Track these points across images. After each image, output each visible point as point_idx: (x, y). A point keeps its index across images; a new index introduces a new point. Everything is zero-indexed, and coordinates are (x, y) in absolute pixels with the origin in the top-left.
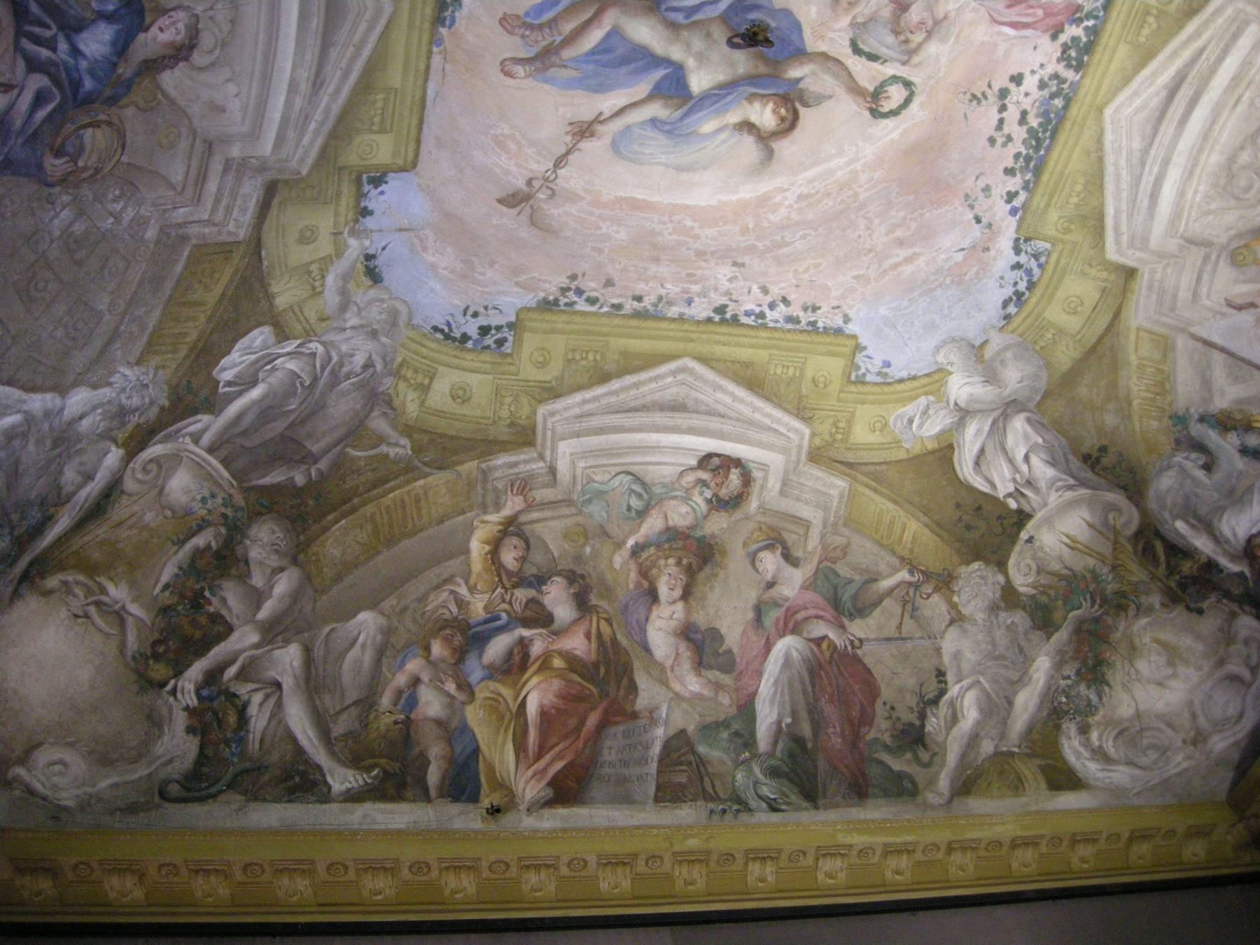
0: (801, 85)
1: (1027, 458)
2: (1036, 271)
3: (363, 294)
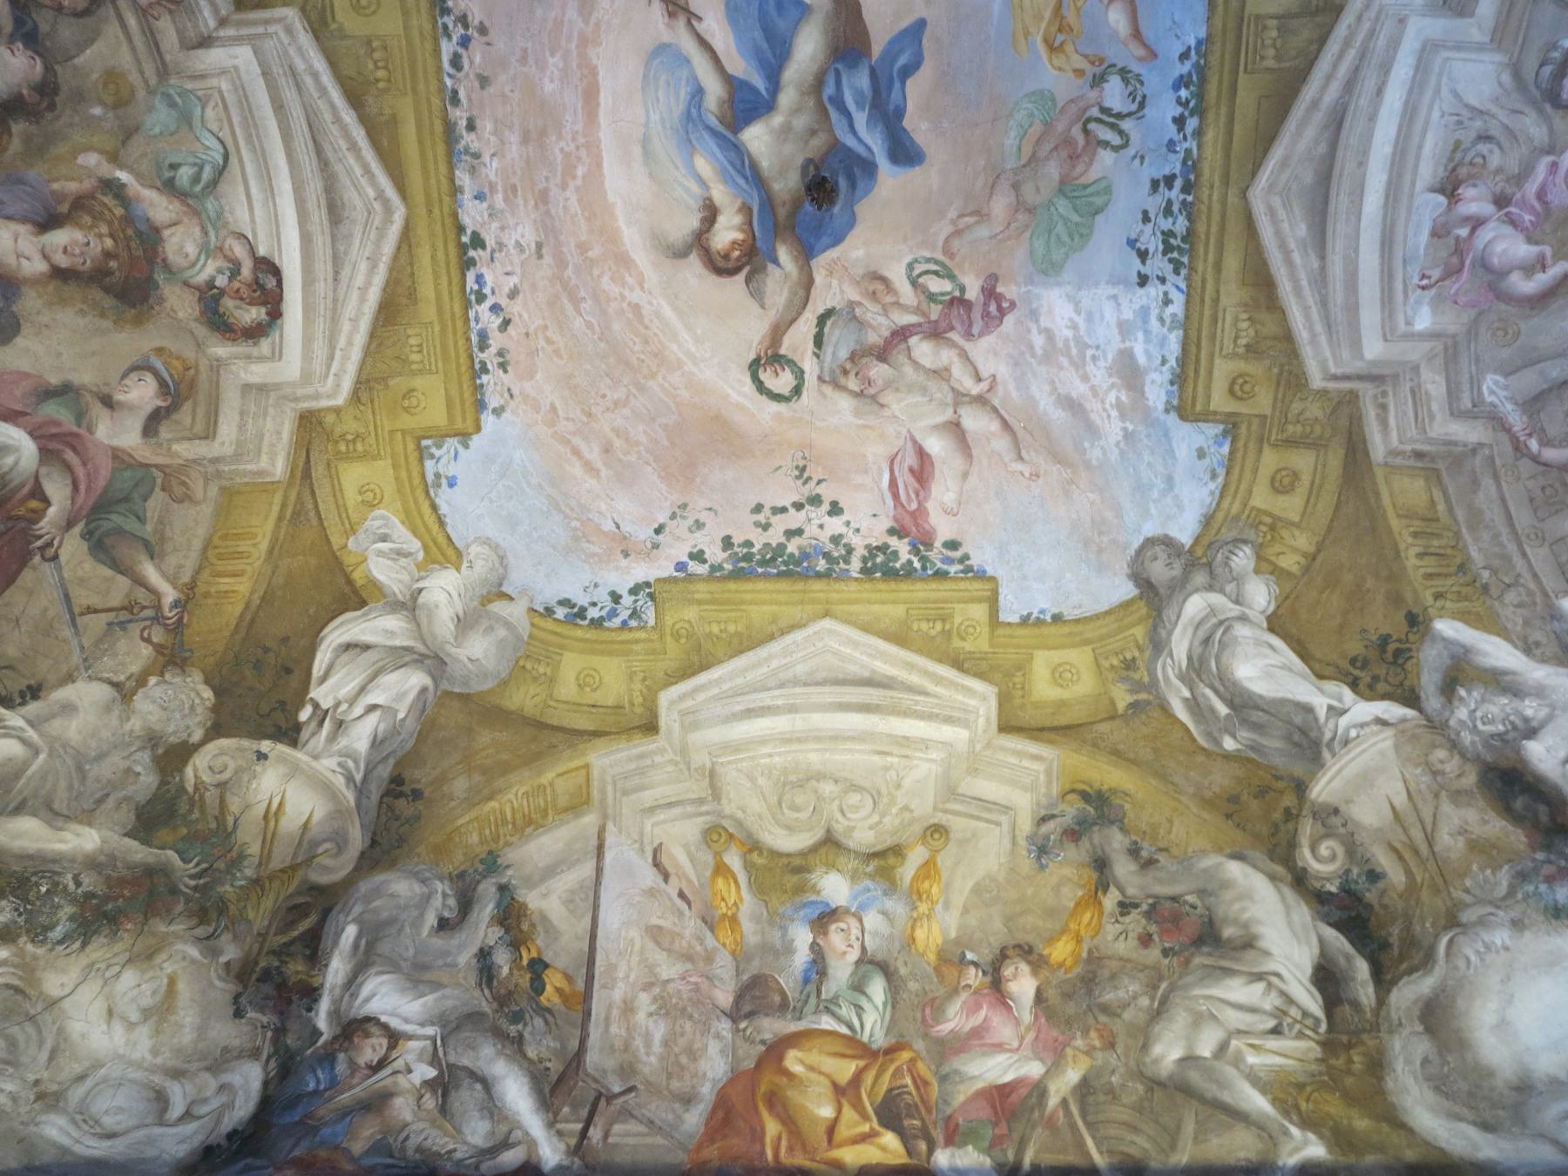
0: (771, 267)
1: (373, 708)
2: (617, 622)
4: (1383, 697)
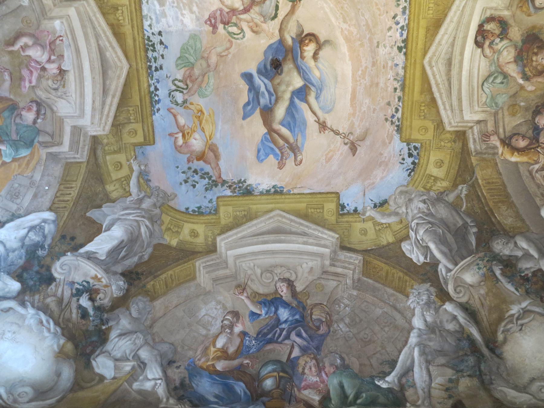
0: (294, 37)
3: (392, 207)
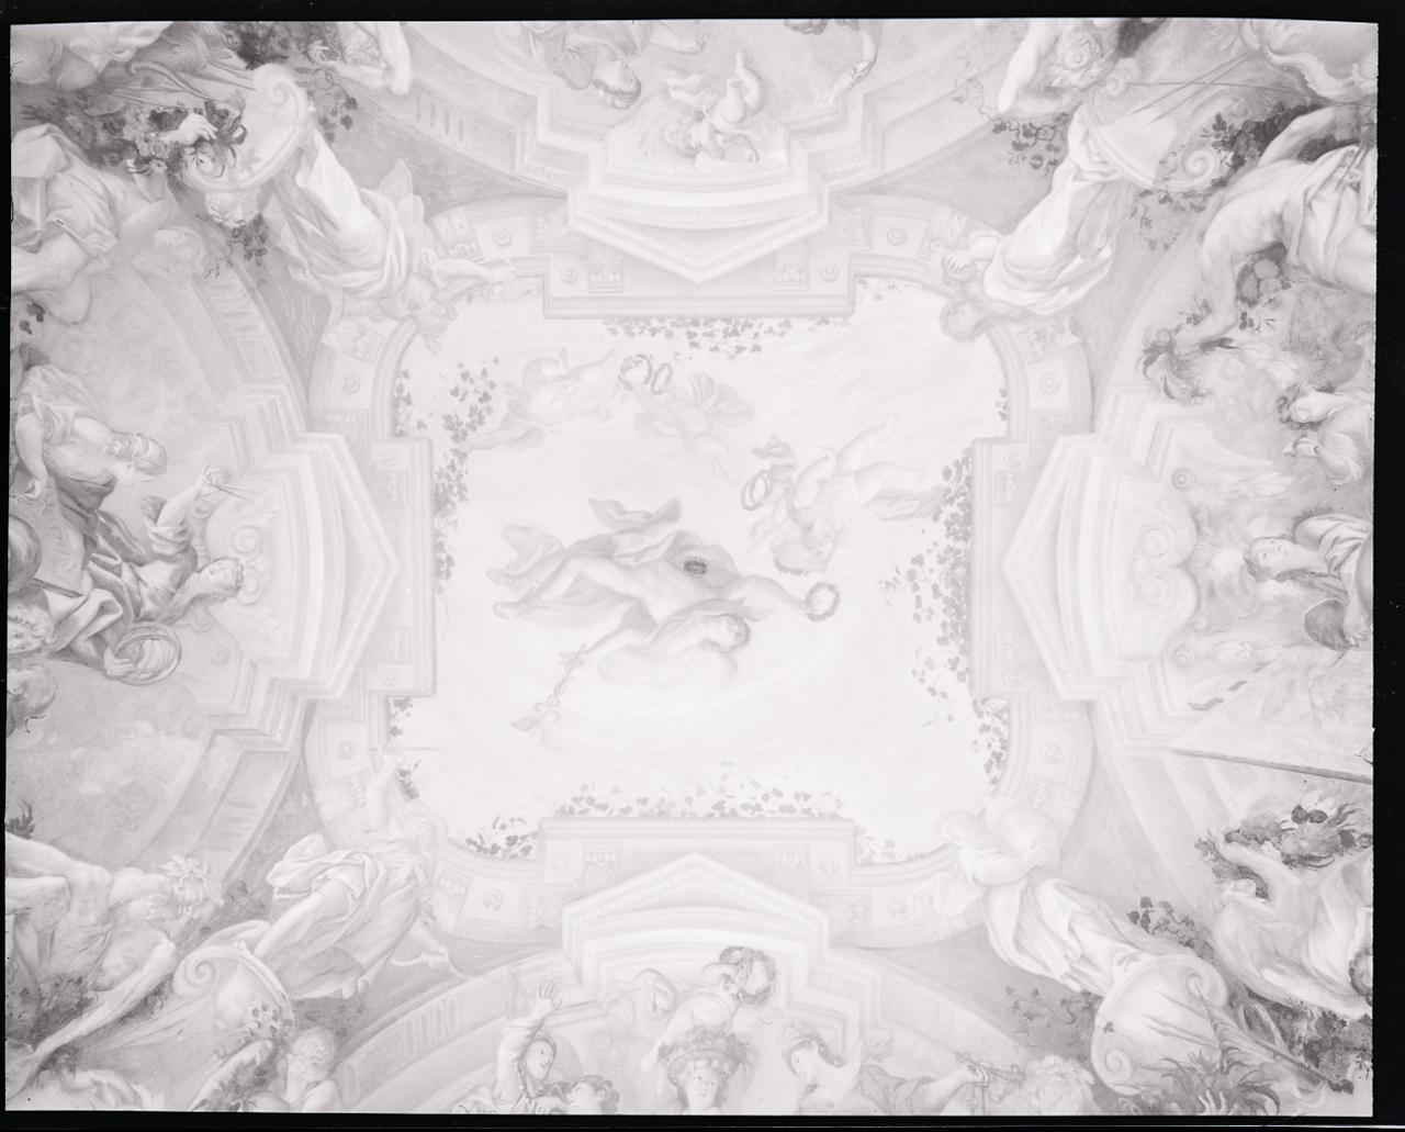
0: (746, 604)
2: (1003, 728)
4: (1064, 138)
